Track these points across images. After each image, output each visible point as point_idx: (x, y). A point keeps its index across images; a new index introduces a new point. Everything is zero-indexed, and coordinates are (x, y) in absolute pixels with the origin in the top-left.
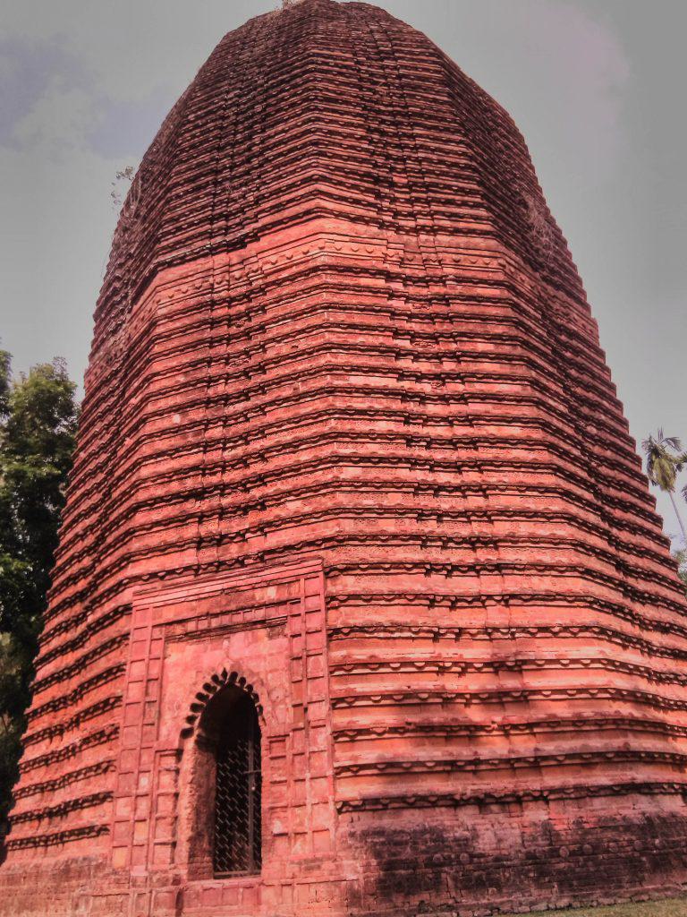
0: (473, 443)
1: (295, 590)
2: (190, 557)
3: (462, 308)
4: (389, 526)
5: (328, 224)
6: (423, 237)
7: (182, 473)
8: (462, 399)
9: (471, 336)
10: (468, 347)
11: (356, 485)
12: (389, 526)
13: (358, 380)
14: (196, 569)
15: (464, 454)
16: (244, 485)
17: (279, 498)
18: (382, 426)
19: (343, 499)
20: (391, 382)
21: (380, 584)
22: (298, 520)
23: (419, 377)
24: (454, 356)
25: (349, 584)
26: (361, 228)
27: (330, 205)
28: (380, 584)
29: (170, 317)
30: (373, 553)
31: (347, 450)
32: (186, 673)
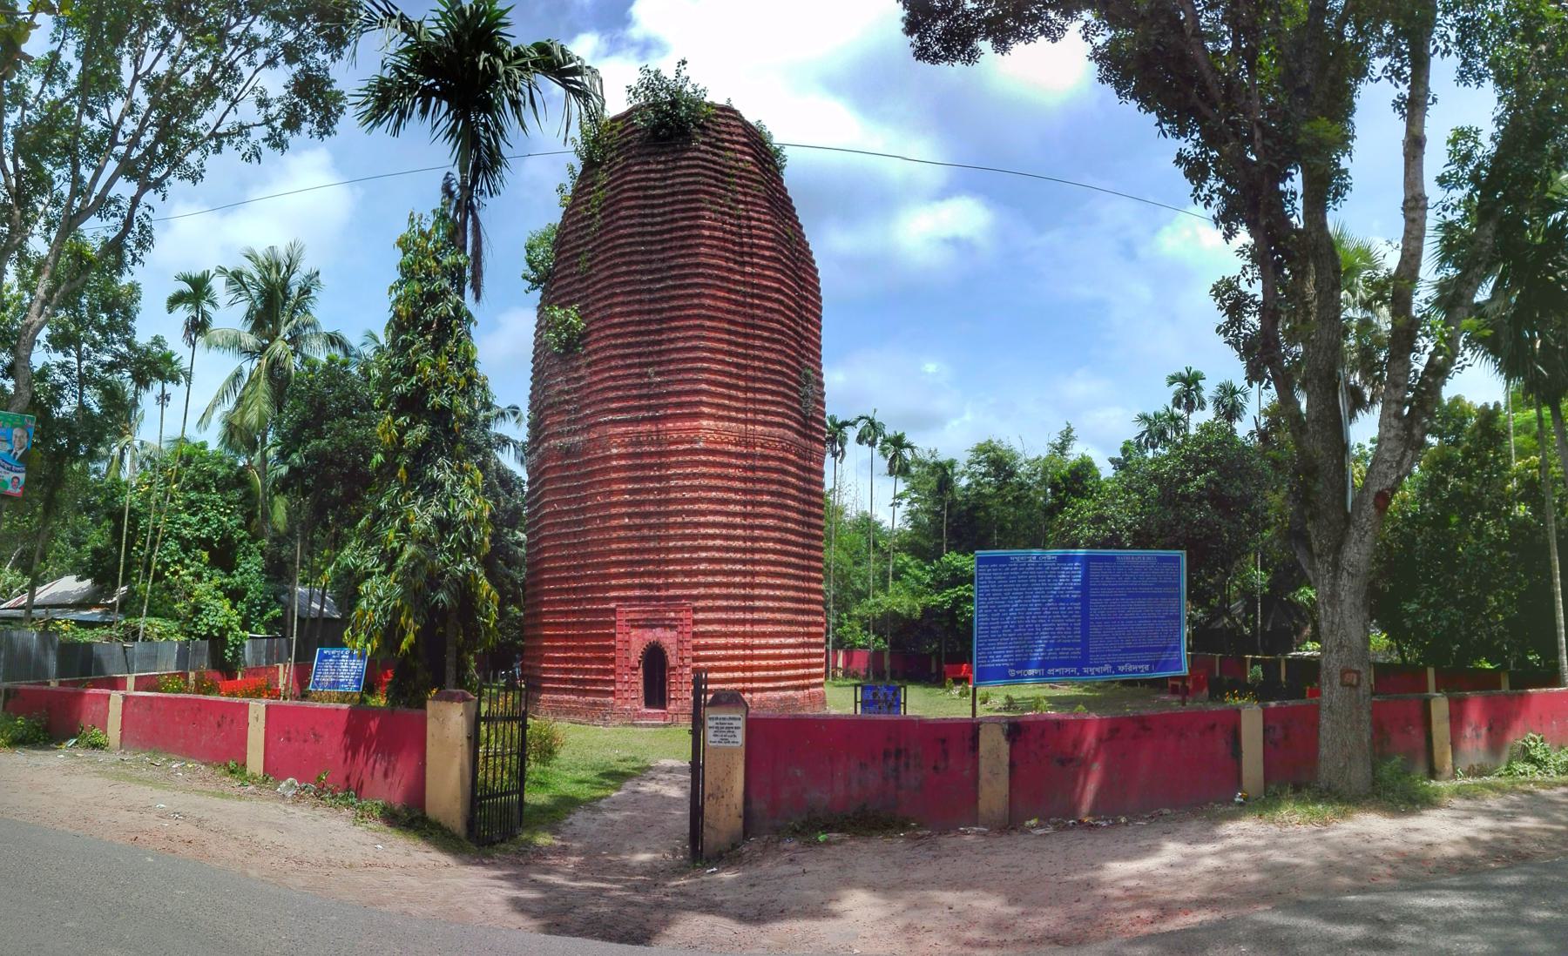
0: (753, 551)
1: (681, 615)
2: (637, 593)
3: (760, 474)
4: (717, 591)
5: (705, 423)
6: (750, 427)
7: (631, 551)
8: (752, 527)
9: (761, 492)
10: (759, 498)
11: (705, 573)
12: (717, 591)
13: (711, 518)
14: (640, 598)
15: (749, 556)
16: (659, 563)
17: (674, 574)
18: (718, 542)
19: (702, 579)
20: (723, 519)
21: (711, 616)
22: (683, 586)
23: (735, 514)
24: (753, 504)
25: (701, 616)
26: (720, 424)
27: (706, 410)
28: (711, 616)
29: (620, 457)
30: (710, 603)
31: (704, 555)
32: (638, 641)
